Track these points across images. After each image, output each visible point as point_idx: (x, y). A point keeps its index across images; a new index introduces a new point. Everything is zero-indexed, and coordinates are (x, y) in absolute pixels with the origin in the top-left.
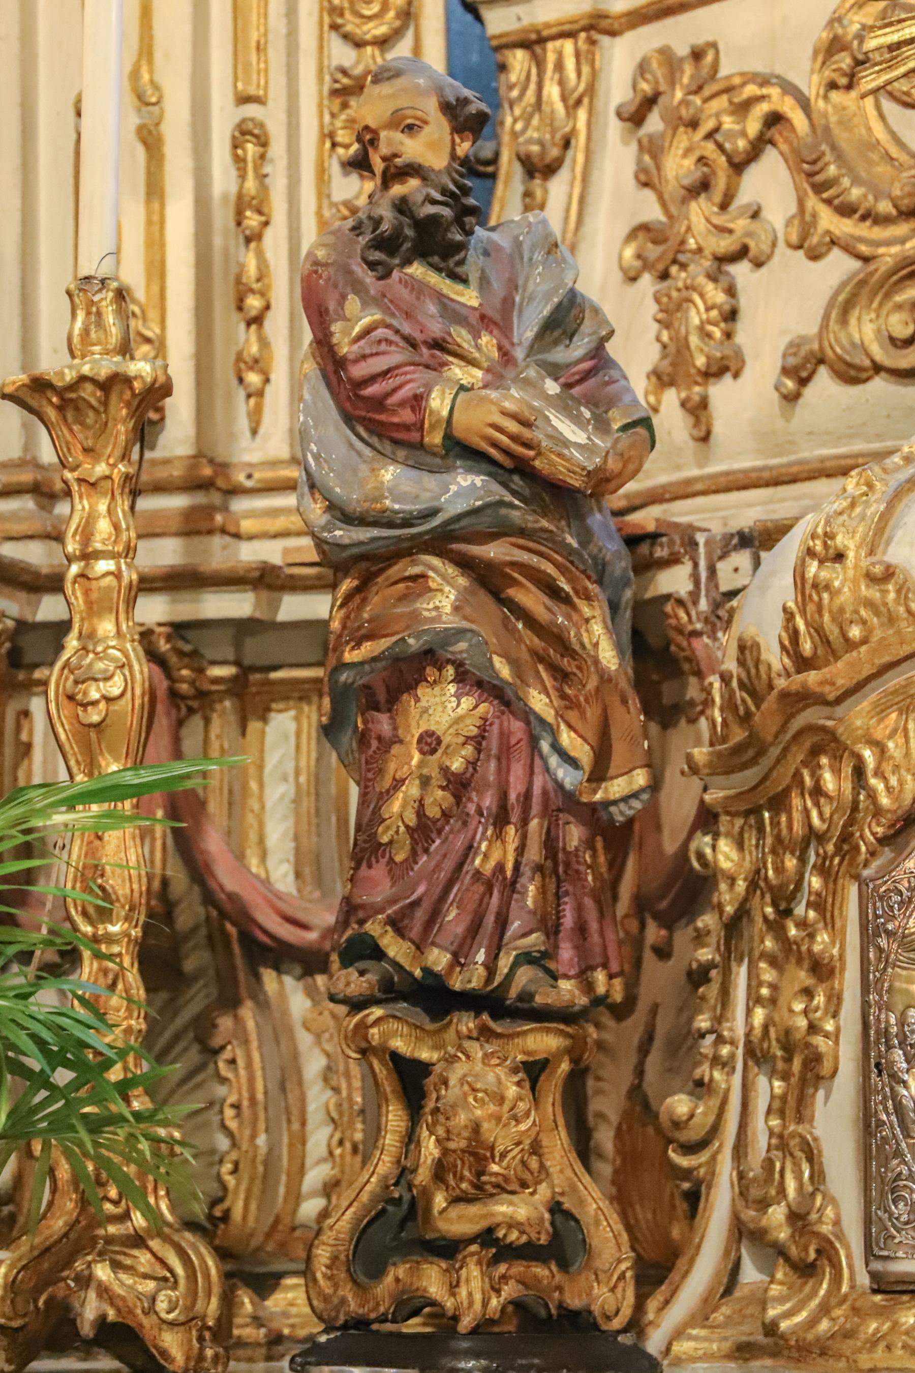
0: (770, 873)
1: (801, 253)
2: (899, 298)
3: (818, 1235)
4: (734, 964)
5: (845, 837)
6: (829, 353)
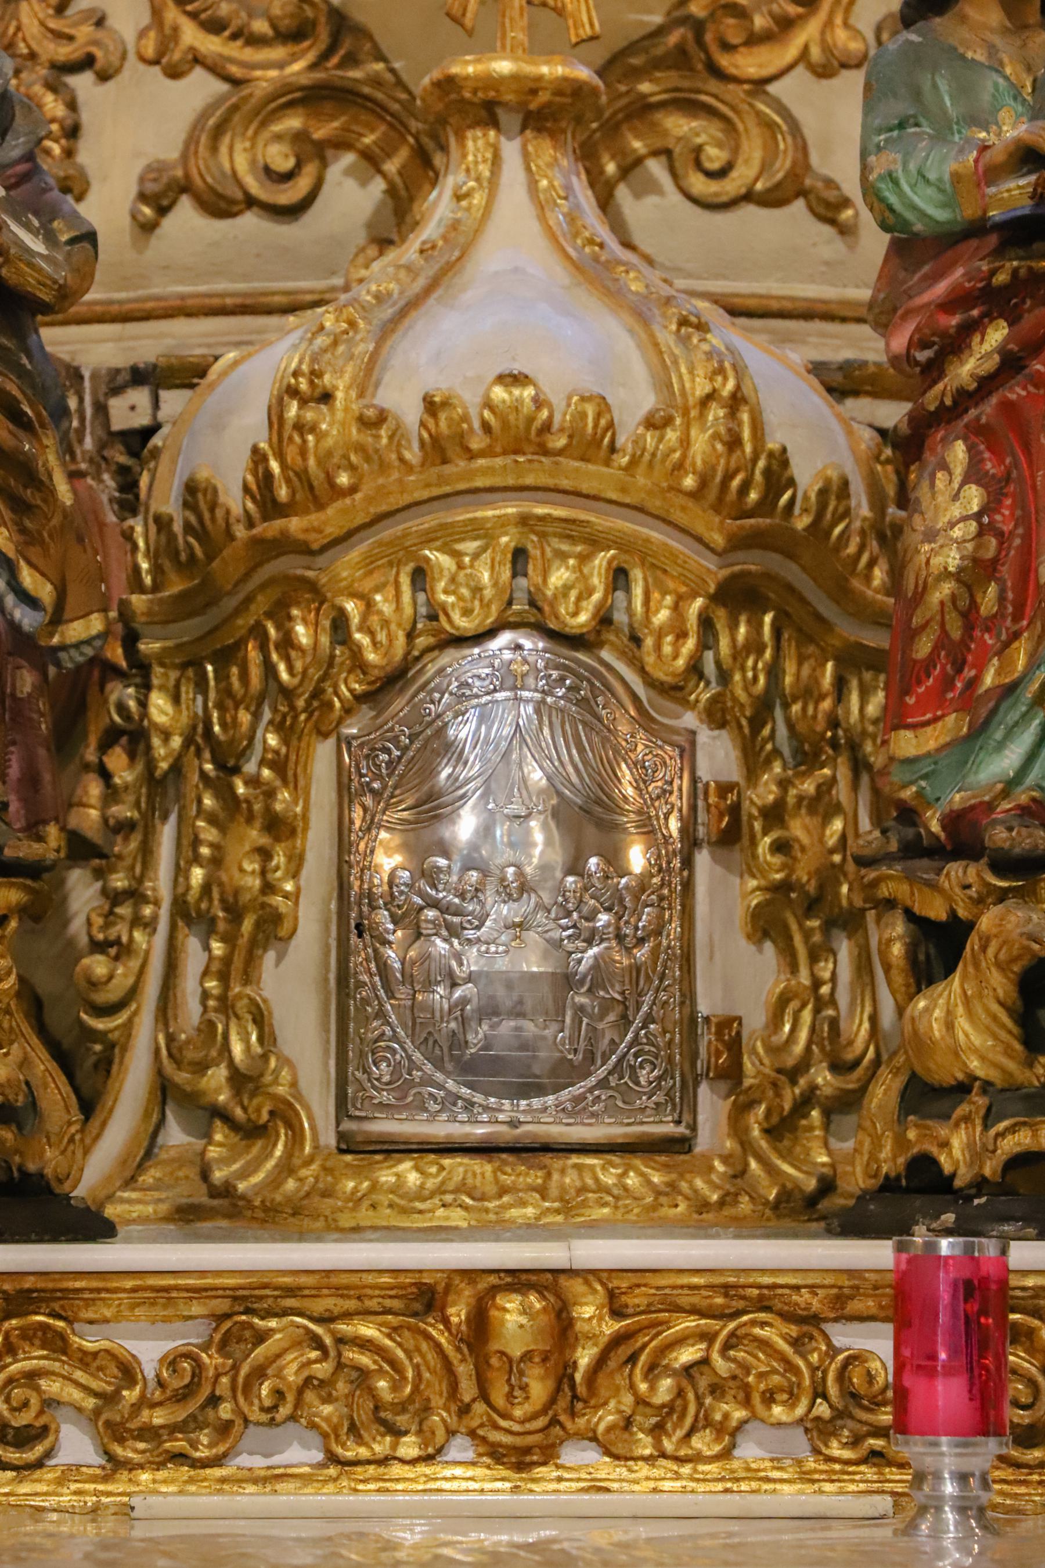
0: (217, 729)
1: (157, 69)
2: (277, 128)
3: (274, 1097)
4: (157, 821)
5: (317, 693)
6: (198, 181)
